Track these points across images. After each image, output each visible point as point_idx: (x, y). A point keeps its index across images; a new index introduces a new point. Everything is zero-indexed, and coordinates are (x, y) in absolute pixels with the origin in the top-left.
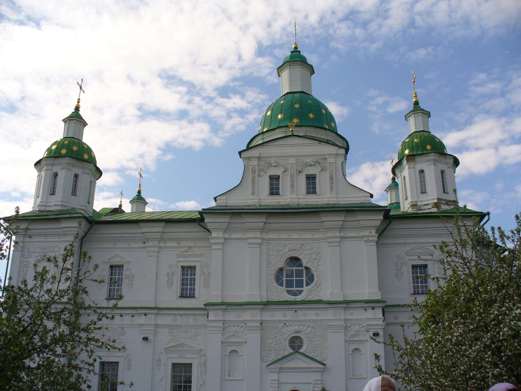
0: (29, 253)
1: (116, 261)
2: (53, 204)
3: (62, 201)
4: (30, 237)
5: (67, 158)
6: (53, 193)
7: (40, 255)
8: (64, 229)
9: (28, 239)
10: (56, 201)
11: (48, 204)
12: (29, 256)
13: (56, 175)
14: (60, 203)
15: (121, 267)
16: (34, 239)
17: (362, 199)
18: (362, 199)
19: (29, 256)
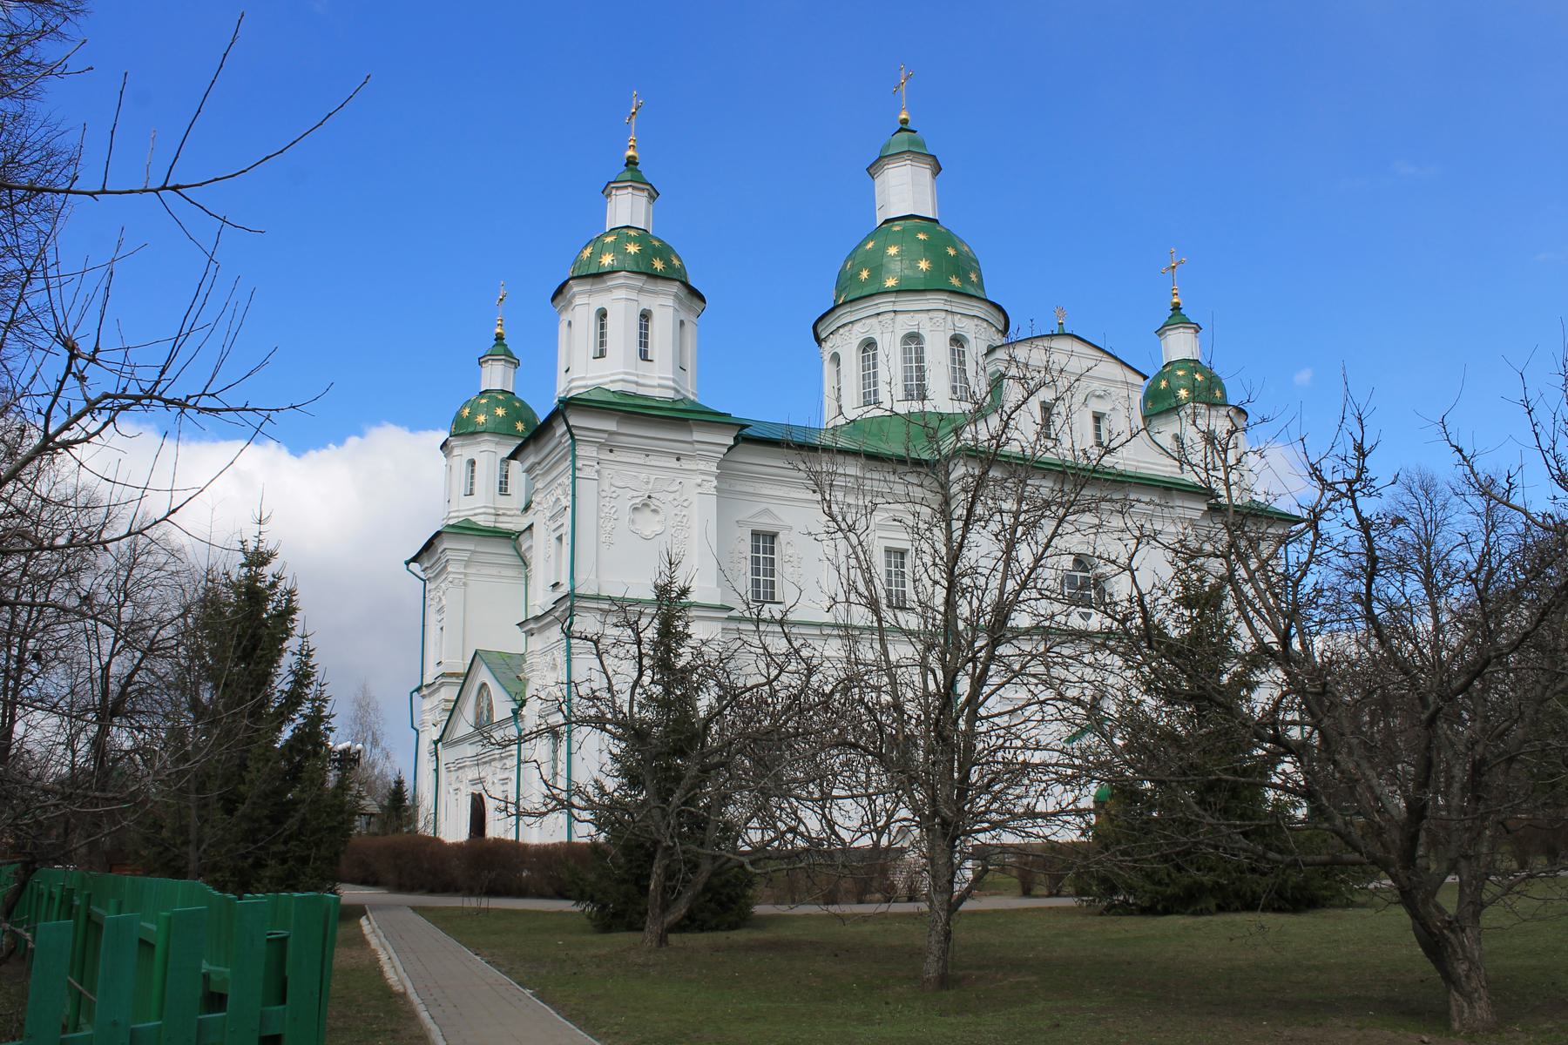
0: (613, 489)
1: (765, 524)
2: (655, 383)
3: (674, 381)
4: (611, 451)
5: (678, 283)
6: (602, 355)
7: (640, 494)
8: (698, 446)
9: (606, 456)
10: (660, 378)
11: (641, 381)
12: (614, 495)
13: (645, 316)
14: (671, 383)
15: (773, 537)
16: (618, 456)
17: (1169, 469)
18: (1169, 469)
19: (614, 495)
